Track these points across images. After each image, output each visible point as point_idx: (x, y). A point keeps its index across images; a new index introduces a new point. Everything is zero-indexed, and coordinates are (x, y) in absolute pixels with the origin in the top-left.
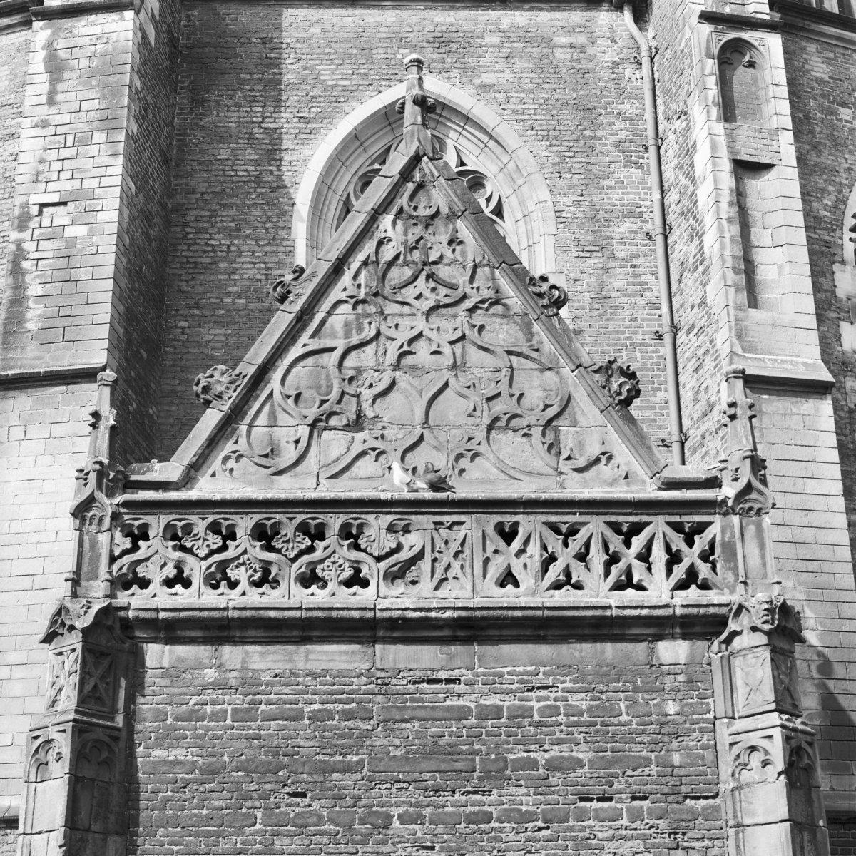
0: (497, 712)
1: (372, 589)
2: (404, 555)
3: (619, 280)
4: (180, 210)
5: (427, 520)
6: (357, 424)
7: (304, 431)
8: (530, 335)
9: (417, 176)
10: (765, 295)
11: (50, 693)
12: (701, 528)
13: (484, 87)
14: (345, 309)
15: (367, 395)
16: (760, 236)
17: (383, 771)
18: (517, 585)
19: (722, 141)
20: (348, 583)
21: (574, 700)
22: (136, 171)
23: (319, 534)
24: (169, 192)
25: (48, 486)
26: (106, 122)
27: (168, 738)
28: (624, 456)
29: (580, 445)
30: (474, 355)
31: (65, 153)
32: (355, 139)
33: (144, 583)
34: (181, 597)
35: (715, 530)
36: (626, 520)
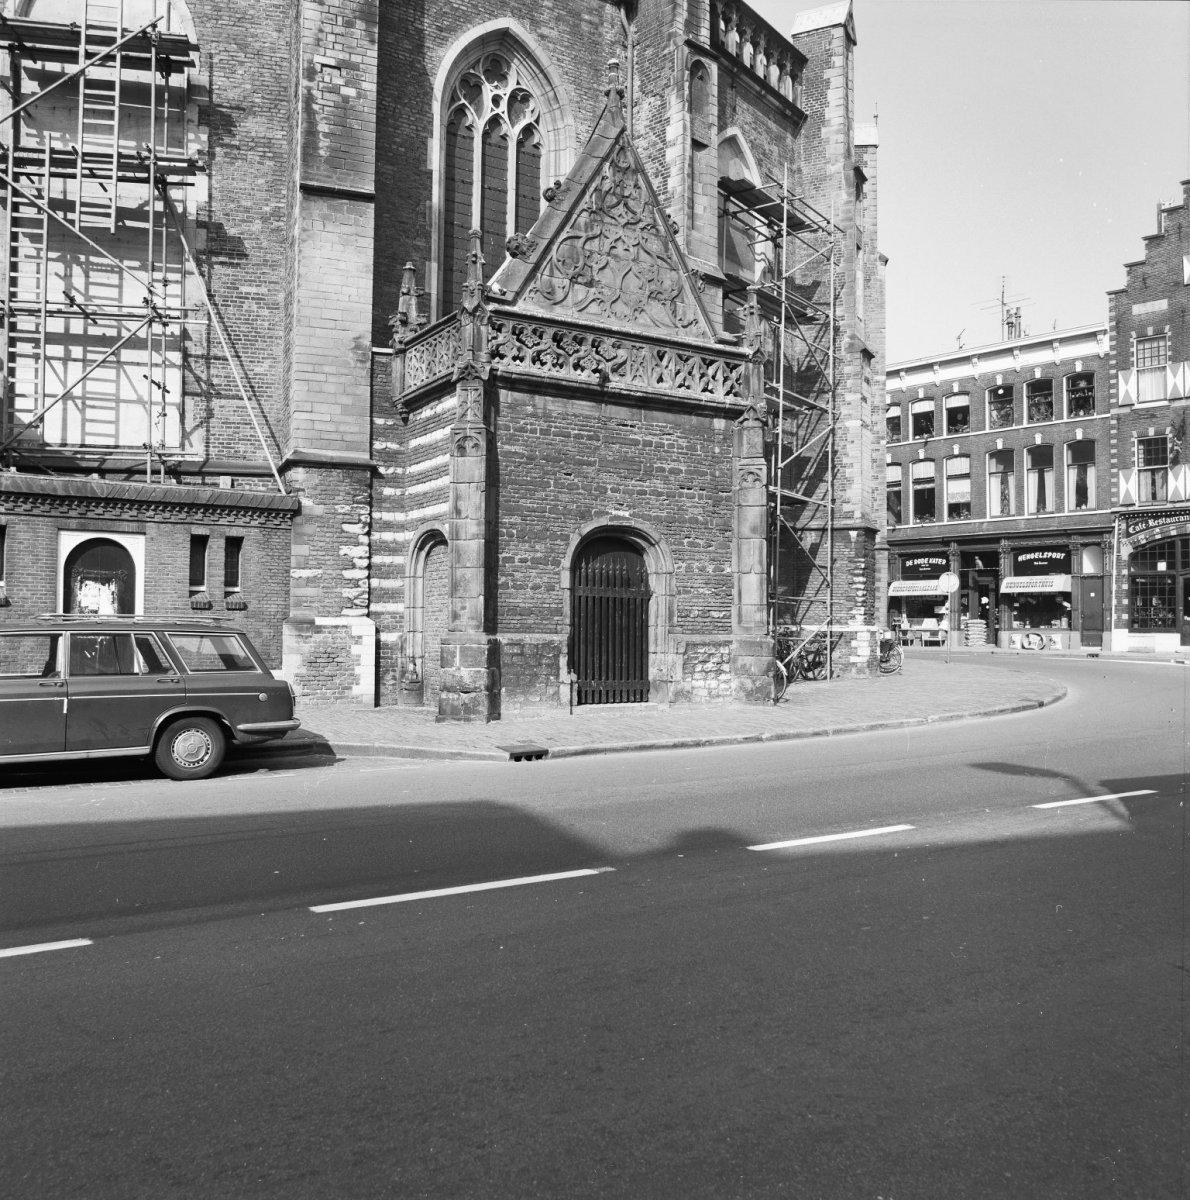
0: (650, 444)
2: (619, 360)
7: (567, 282)
12: (736, 366)
13: (543, 37)
15: (596, 267)
17: (605, 466)
25: (342, 265)
27: (511, 440)
29: (684, 314)
31: (337, 30)
35: (742, 369)
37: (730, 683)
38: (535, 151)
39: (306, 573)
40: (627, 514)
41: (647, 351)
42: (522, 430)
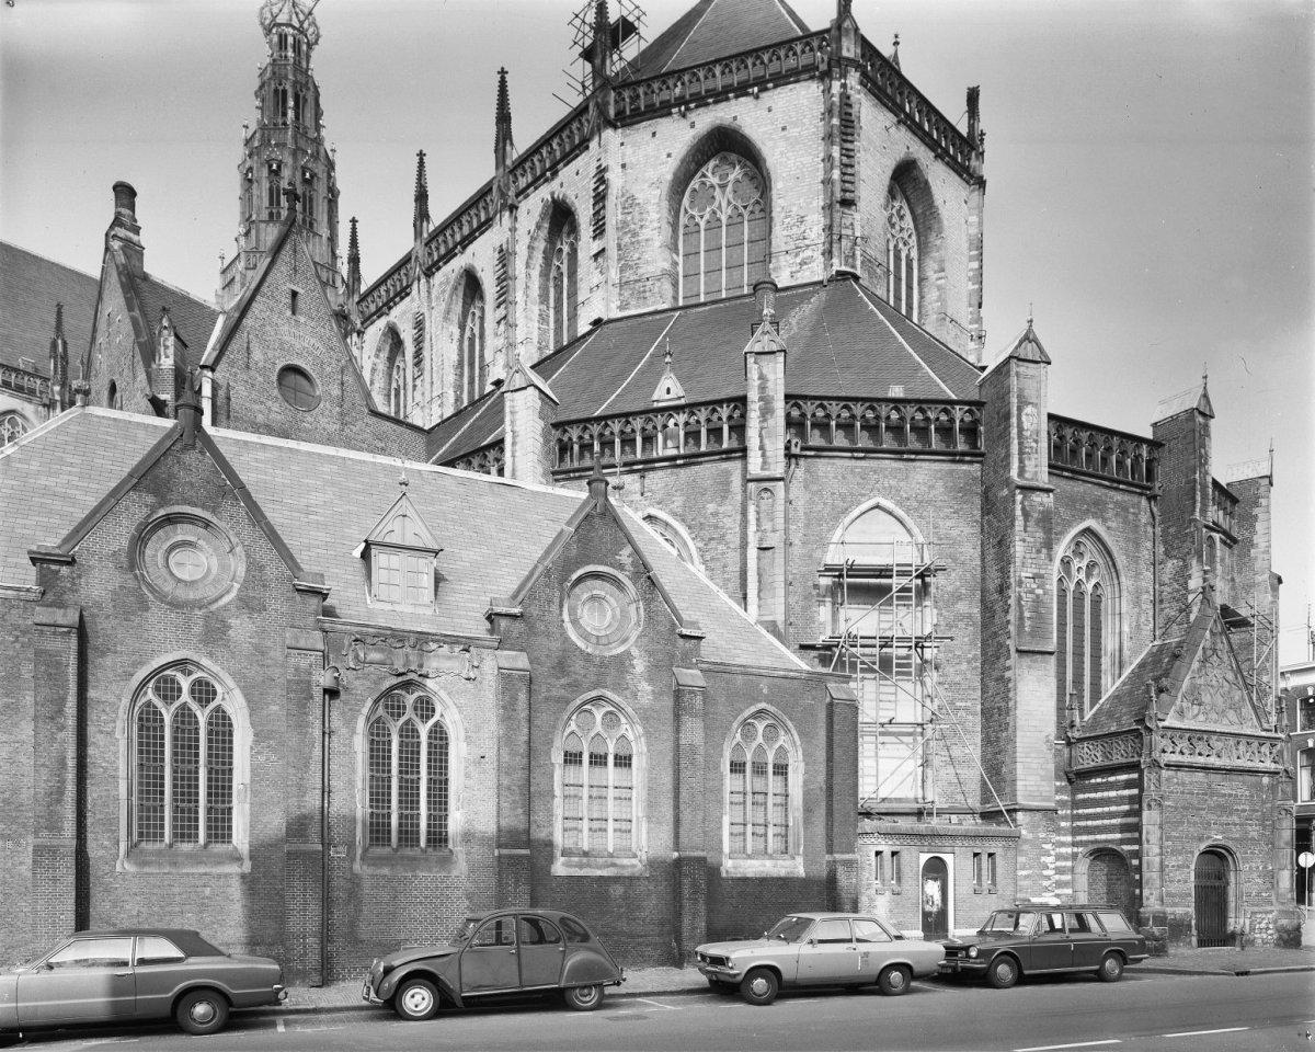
13: (1108, 528)
39: (1024, 873)
40: (1220, 837)
41: (1232, 741)
42: (1172, 792)
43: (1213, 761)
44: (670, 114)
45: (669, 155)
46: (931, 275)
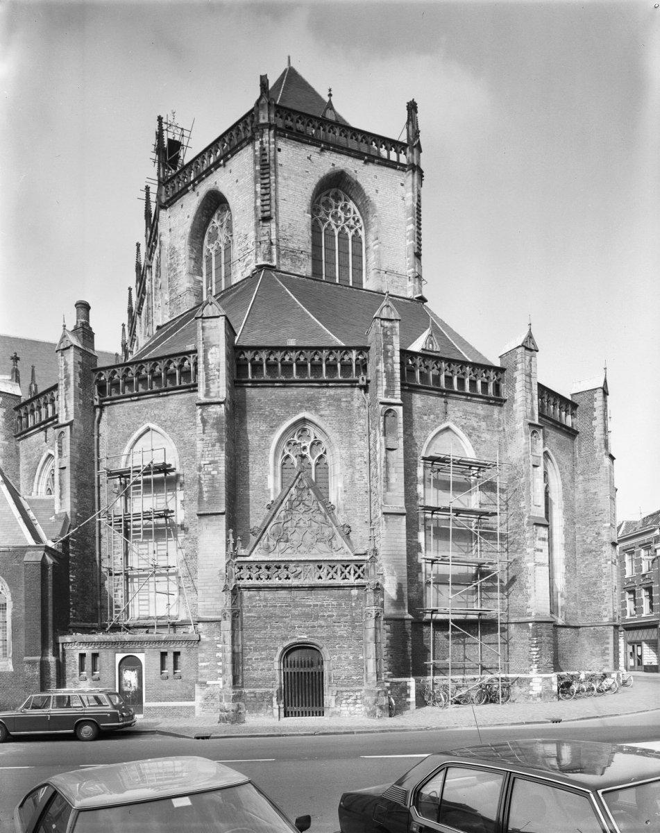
0: (317, 605)
1: (290, 580)
2: (297, 572)
3: (357, 476)
4: (238, 456)
5: (302, 565)
6: (287, 541)
7: (275, 542)
8: (326, 519)
9: (300, 476)
10: (392, 487)
11: (225, 602)
12: (362, 566)
13: (321, 416)
14: (283, 512)
15: (289, 534)
16: (392, 470)
17: (294, 617)
18: (322, 578)
19: (383, 442)
20: (286, 579)
21: (333, 603)
22: (228, 453)
23: (279, 568)
24: (235, 451)
25: (214, 542)
26: (220, 440)
27: (250, 611)
28: (346, 548)
29: (337, 545)
30: (313, 523)
31: (209, 449)
32: (286, 432)
33: (243, 579)
34: (250, 582)
35: (364, 566)
36: (345, 564)
37: (360, 709)
38: (325, 466)
39: (204, 664)
40: (306, 637)
41: (311, 566)
42: (254, 606)
43: (294, 582)
44: (188, 191)
45: (188, 217)
46: (371, 244)
